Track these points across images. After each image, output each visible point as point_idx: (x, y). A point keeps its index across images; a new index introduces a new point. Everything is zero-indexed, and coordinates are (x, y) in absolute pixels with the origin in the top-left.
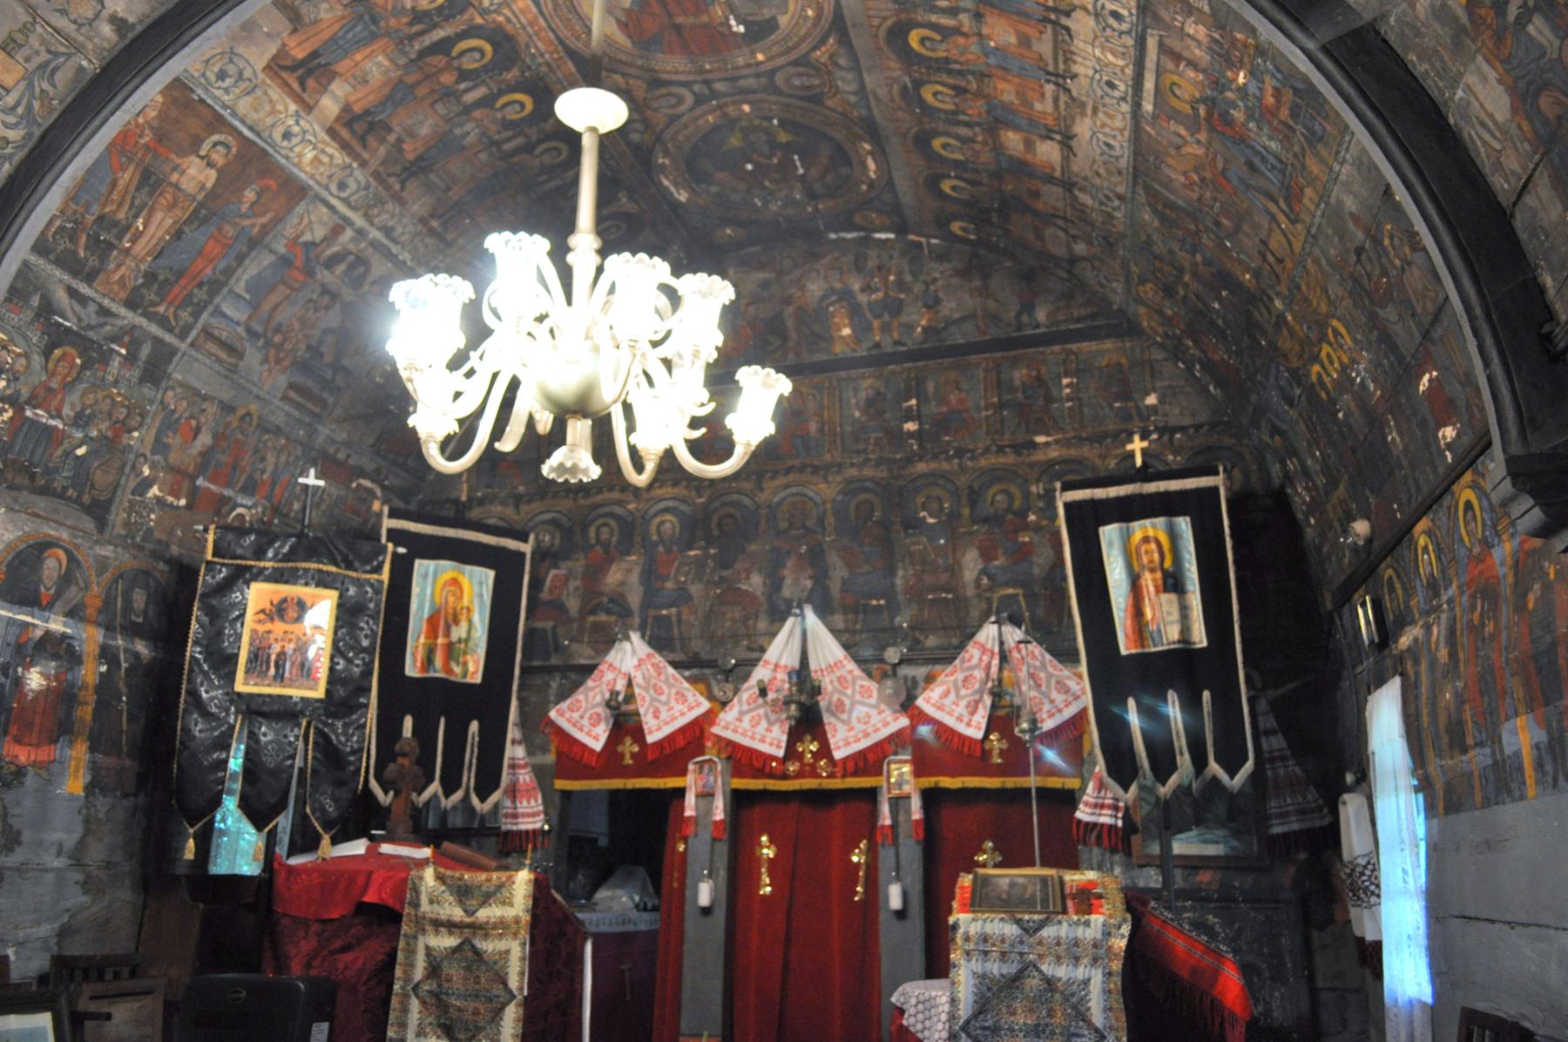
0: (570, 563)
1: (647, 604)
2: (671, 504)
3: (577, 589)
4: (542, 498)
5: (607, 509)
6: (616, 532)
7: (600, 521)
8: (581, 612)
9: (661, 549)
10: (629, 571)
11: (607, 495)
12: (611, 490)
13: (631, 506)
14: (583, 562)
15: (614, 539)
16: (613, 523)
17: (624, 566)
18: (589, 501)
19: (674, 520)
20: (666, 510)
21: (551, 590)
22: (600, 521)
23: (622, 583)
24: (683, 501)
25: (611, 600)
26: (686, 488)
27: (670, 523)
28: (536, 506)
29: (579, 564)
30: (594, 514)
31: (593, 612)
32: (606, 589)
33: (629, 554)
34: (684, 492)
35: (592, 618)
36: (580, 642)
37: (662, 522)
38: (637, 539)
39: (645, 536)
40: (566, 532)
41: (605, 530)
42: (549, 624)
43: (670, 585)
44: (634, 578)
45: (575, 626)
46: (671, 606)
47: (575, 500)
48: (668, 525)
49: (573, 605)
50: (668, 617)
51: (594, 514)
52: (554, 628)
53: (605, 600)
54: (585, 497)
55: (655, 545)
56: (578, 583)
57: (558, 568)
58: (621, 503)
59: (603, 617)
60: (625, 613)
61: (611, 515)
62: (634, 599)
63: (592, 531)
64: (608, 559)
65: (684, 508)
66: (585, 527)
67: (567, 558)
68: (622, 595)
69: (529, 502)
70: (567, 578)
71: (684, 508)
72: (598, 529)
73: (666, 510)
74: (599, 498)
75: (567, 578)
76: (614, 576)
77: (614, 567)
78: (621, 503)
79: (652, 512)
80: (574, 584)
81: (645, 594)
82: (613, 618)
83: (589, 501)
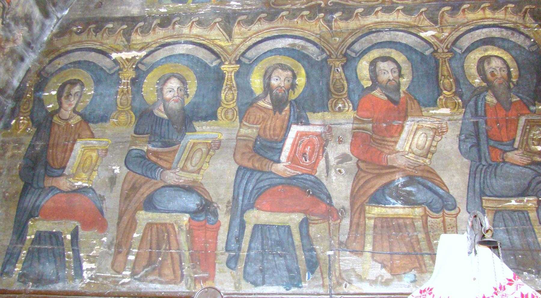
0: (328, 117)
1: (478, 191)
2: (495, 33)
3: (344, 158)
4: (272, 17)
5: (386, 37)
6: (406, 68)
7: (375, 53)
8: (354, 197)
9: (490, 99)
10: (438, 132)
11: (383, 17)
12: (389, 10)
13: (427, 34)
14: (351, 114)
15: (405, 81)
16: (400, 58)
17: (427, 124)
18: (353, 24)
19: (507, 57)
20: (488, 41)
21: (293, 160)
22: (375, 53)
23: (428, 152)
24: (515, 30)
25: (411, 180)
26: (515, 12)
27: (499, 60)
28: (261, 28)
29: (345, 119)
30: (364, 43)
31: (377, 199)
32: (401, 162)
33: (434, 105)
34: (514, 18)
35: (376, 211)
36: (359, 252)
37: (482, 60)
38: (446, 82)
39: (460, 79)
40: (318, 68)
41: (382, 65)
42: (294, 219)
43: (515, 156)
44: (449, 143)
45: (346, 222)
46: (524, 193)
47: (328, 22)
48: (495, 64)
49: (339, 187)
50: (522, 212)
51: (364, 43)
52: (305, 224)
53: (400, 179)
54: (341, 19)
55: (478, 93)
56: (345, 148)
57: (307, 123)
58: (407, 29)
59: (396, 209)
60: (444, 203)
61: (391, 44)
62: (455, 179)
63: (363, 68)
64: (398, 109)
65: (519, 40)
66: (349, 61)
67: (324, 108)
68: (431, 171)
69: (250, 22)
70: (324, 140)
71: (519, 40)
72: (373, 64)
73: (488, 41)
74: (370, 20)
75: (324, 140)
76: (411, 140)
77: (409, 125)
78: (407, 29)
79: (466, 42)
80: (335, 151)
81: (473, 175)
82: (418, 211)
83: (353, 24)
